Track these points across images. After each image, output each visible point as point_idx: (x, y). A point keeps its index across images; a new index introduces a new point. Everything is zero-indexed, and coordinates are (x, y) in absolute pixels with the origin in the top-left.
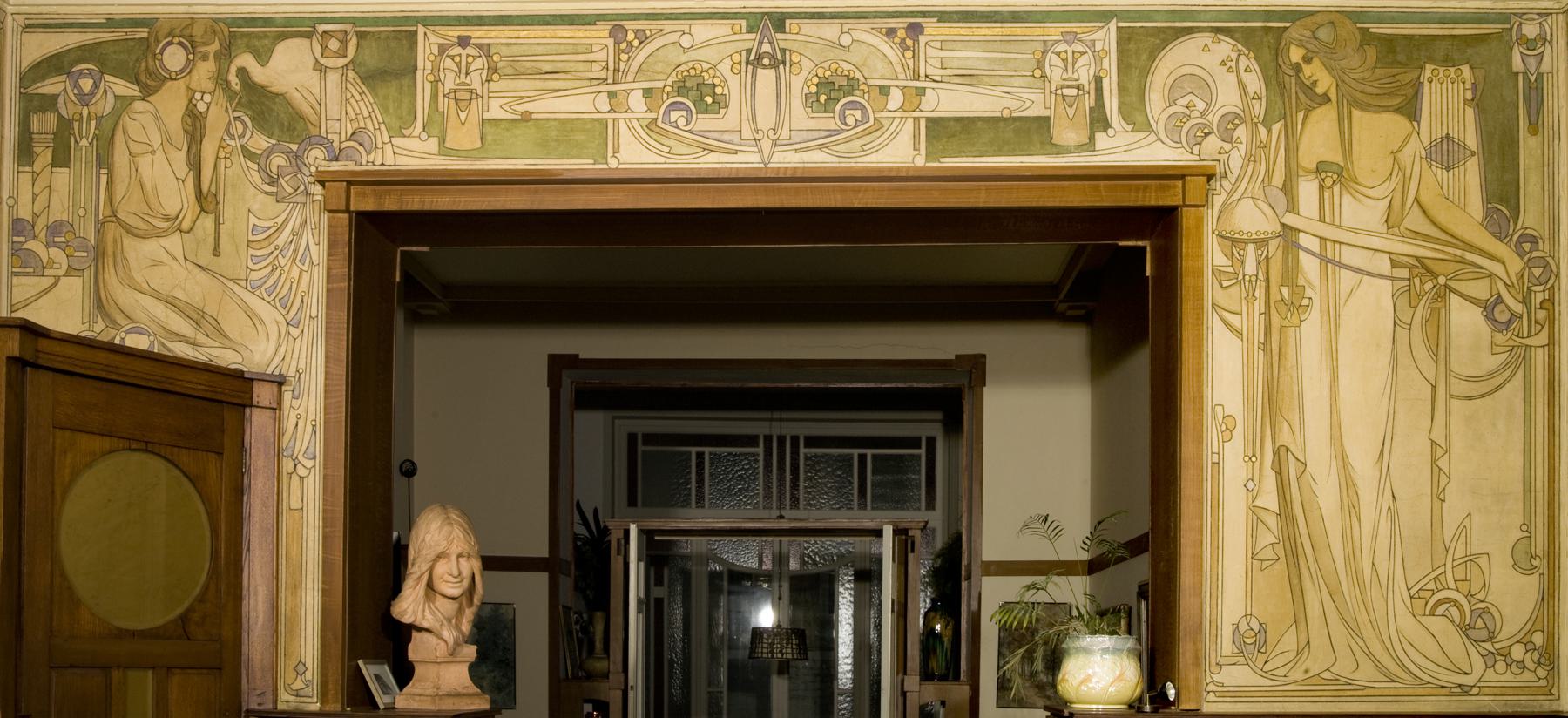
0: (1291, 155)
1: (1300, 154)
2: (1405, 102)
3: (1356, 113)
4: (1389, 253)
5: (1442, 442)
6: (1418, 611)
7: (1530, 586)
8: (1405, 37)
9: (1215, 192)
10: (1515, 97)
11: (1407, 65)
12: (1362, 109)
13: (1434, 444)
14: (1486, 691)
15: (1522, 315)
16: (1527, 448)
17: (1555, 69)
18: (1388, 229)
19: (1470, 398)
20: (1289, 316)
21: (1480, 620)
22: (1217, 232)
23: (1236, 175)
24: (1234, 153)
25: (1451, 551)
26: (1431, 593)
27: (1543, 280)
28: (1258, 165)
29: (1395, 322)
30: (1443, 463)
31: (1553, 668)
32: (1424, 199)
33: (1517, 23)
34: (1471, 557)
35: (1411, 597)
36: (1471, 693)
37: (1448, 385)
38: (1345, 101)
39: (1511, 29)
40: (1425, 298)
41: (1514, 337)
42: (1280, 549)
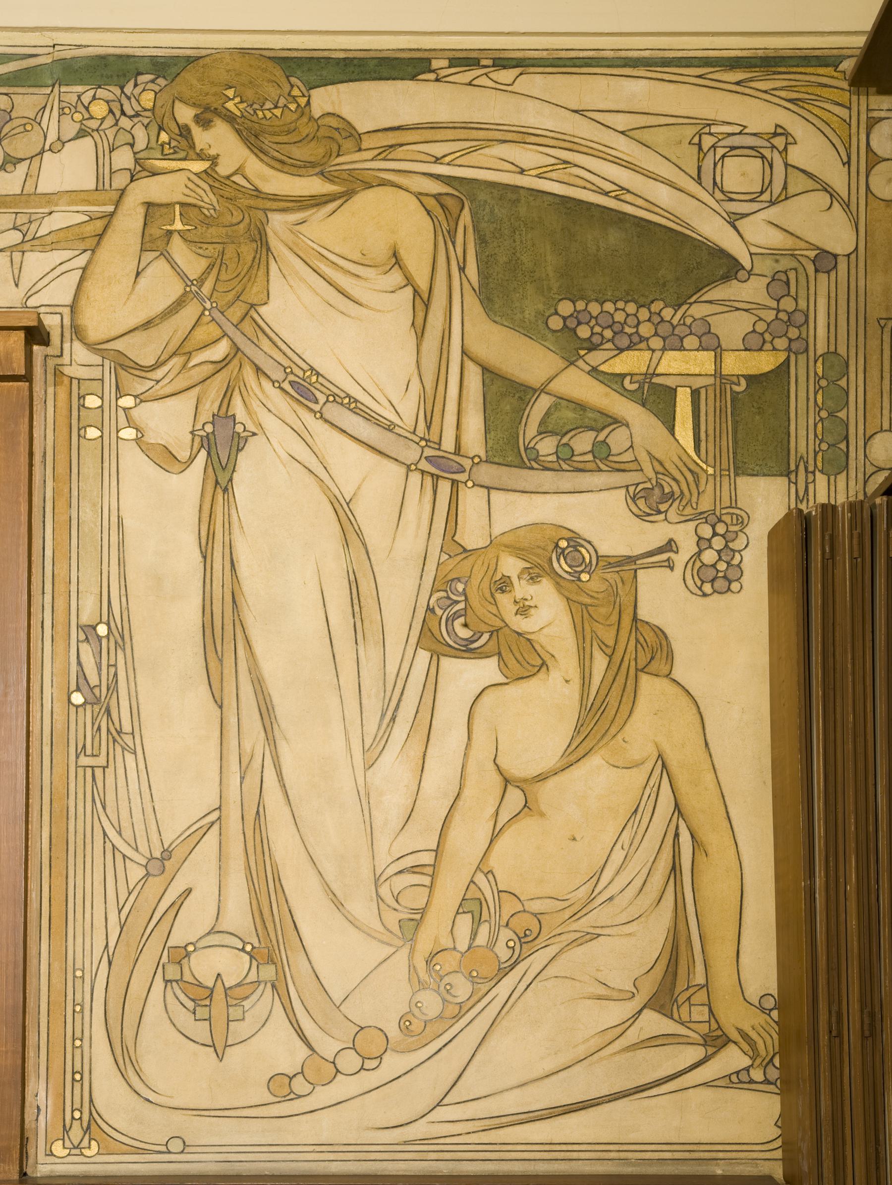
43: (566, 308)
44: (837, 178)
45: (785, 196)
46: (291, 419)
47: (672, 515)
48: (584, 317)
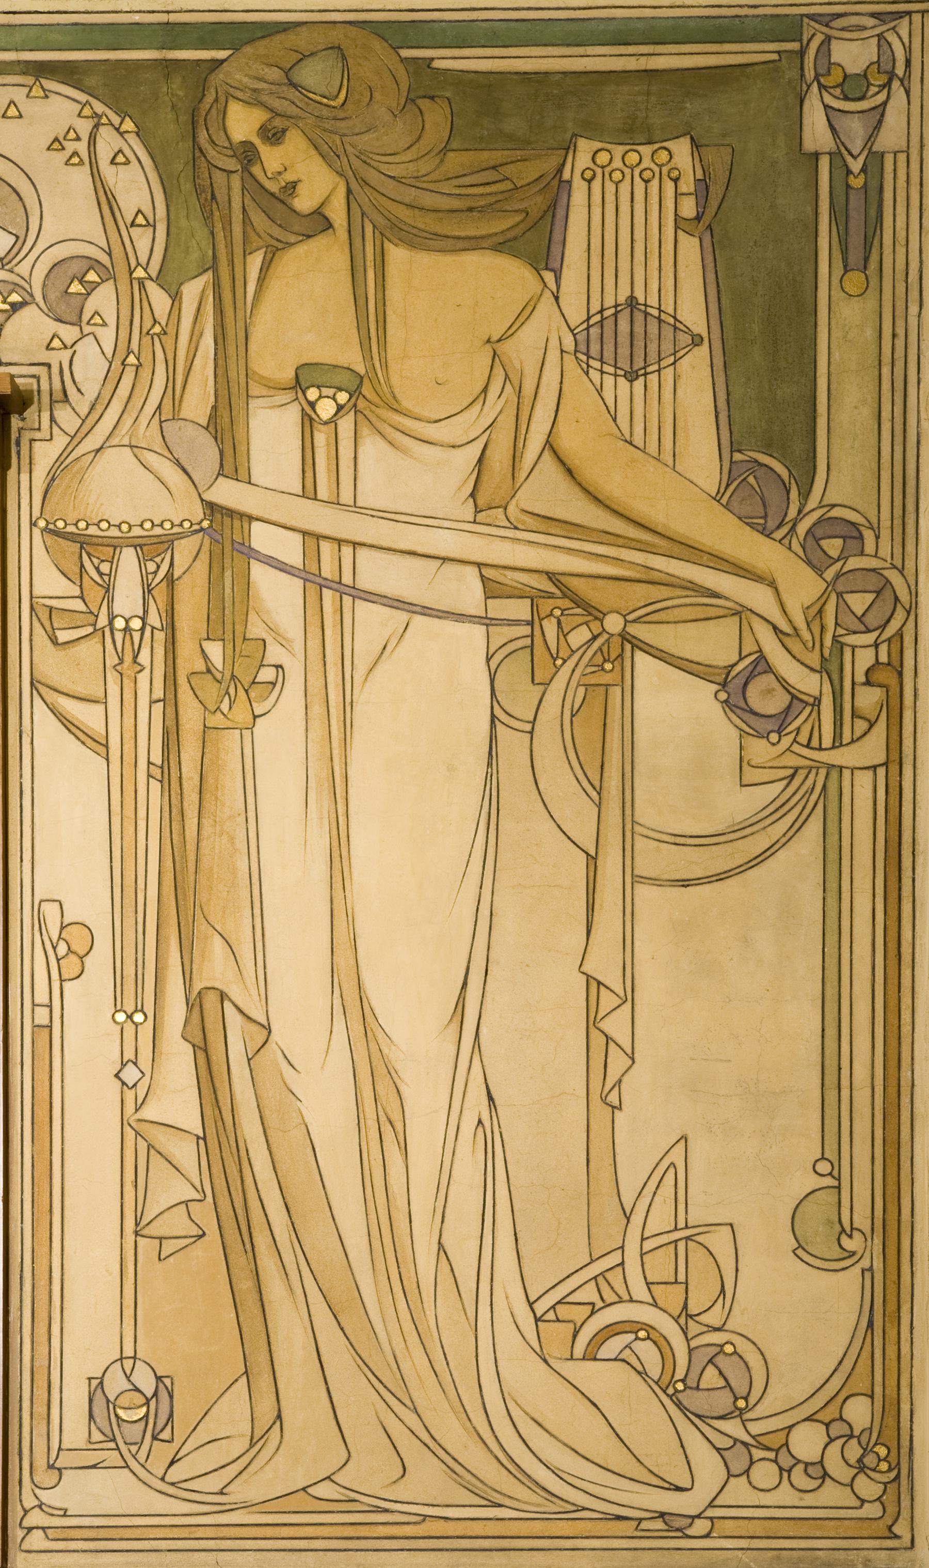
0: (231, 350)
1: (253, 347)
2: (522, 227)
3: (397, 255)
4: (479, 565)
5: (613, 979)
8: (525, 77)
9: (37, 435)
10: (809, 209)
11: (529, 143)
12: (412, 246)
13: (594, 985)
14: (729, 1527)
15: (817, 701)
16: (831, 992)
17: (915, 140)
18: (477, 511)
19: (685, 883)
20: (225, 706)
21: (711, 1371)
22: (42, 523)
23: (91, 395)
24: (87, 348)
25: (637, 1220)
26: (588, 1309)
27: (873, 620)
28: (145, 373)
29: (493, 716)
30: (618, 1026)
31: (898, 1477)
32: (568, 442)
33: (819, 39)
34: (688, 1233)
35: (537, 1320)
36: (689, 1532)
37: (628, 852)
38: (369, 229)
39: (802, 53)
40: (570, 664)
41: (796, 748)
42: (205, 1215)
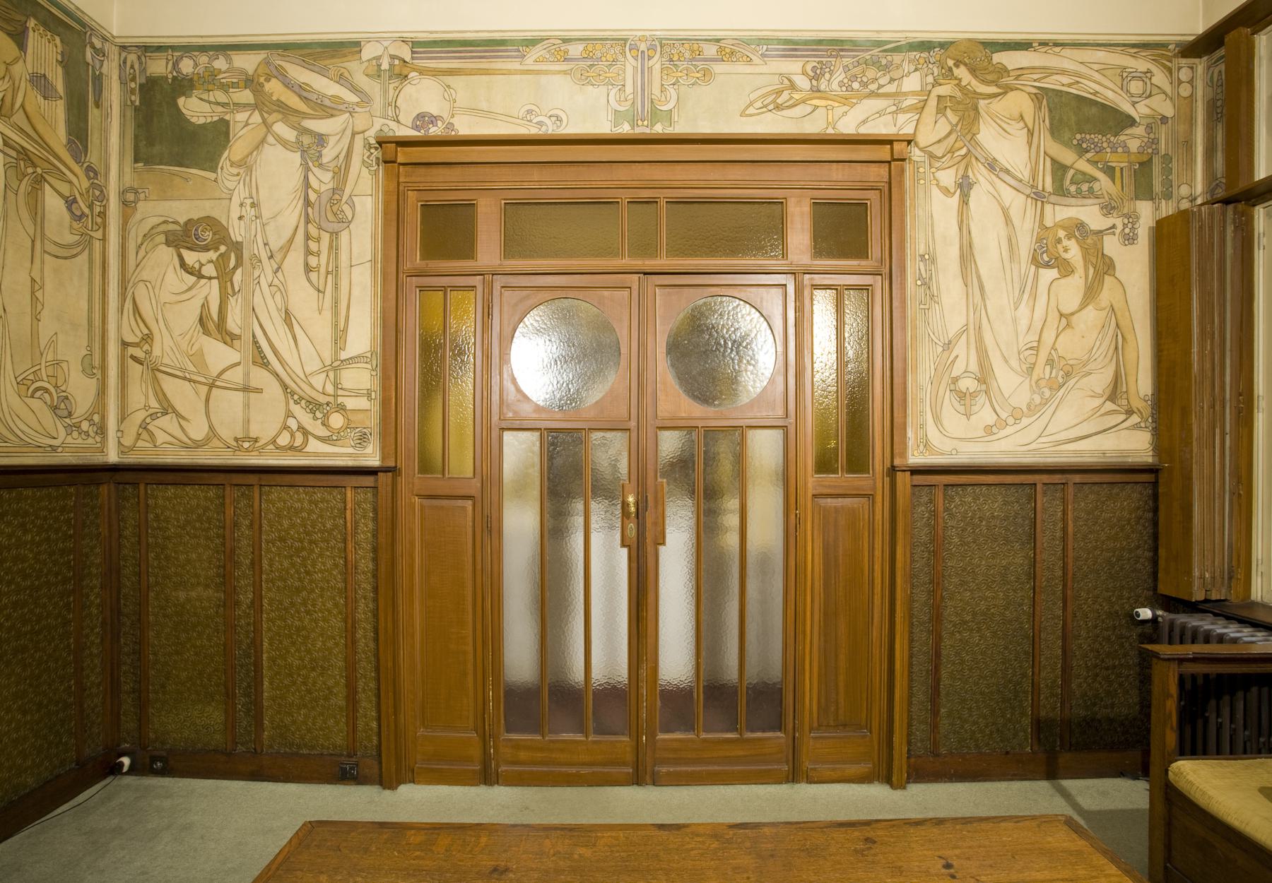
5: (38, 280)
6: (23, 394)
7: (92, 384)
13: (33, 280)
14: (67, 449)
19: (57, 257)
25: (44, 356)
30: (39, 294)
32: (28, 108)
37: (42, 242)
43: (1078, 136)
44: (1168, 88)
45: (1150, 96)
46: (988, 177)
47: (1115, 215)
48: (1084, 140)
